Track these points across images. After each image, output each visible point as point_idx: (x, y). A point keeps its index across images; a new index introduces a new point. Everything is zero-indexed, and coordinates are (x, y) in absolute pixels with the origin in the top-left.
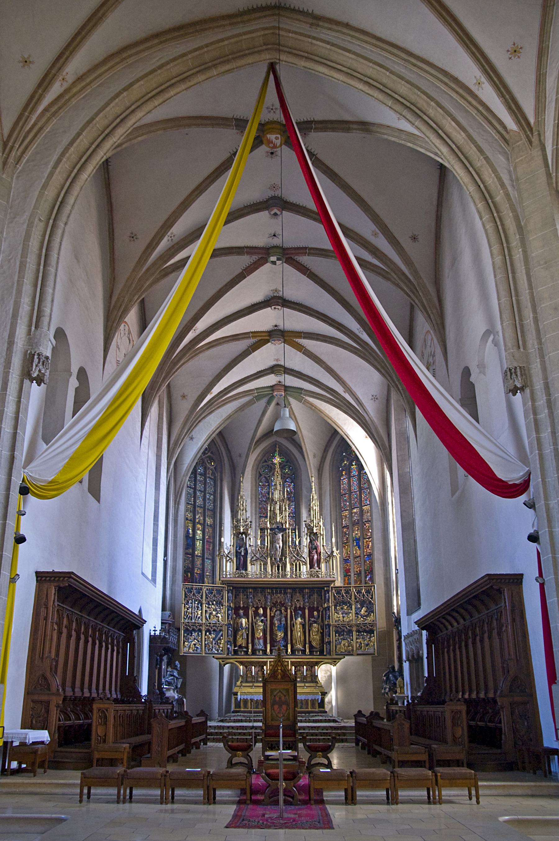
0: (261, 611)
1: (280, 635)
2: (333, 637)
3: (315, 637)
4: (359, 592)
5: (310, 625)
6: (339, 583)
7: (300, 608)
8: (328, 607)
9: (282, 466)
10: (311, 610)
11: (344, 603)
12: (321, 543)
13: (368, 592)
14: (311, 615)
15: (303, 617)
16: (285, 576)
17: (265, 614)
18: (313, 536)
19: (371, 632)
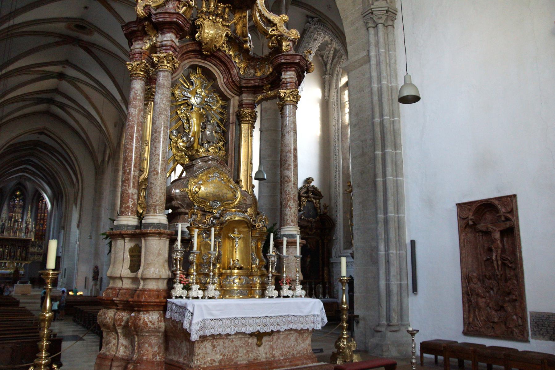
0: (7, 247)
1: (13, 254)
2: (30, 256)
3: (24, 255)
4: (39, 243)
5: (23, 252)
6: (33, 240)
7: (21, 247)
8: (29, 247)
9: (20, 195)
10: (24, 247)
11: (34, 246)
12: (30, 227)
13: (42, 243)
14: (23, 249)
15: (21, 249)
16: (16, 236)
17: (8, 248)
18: (27, 225)
19: (41, 255)
